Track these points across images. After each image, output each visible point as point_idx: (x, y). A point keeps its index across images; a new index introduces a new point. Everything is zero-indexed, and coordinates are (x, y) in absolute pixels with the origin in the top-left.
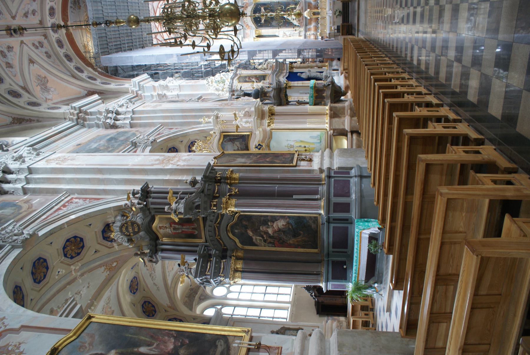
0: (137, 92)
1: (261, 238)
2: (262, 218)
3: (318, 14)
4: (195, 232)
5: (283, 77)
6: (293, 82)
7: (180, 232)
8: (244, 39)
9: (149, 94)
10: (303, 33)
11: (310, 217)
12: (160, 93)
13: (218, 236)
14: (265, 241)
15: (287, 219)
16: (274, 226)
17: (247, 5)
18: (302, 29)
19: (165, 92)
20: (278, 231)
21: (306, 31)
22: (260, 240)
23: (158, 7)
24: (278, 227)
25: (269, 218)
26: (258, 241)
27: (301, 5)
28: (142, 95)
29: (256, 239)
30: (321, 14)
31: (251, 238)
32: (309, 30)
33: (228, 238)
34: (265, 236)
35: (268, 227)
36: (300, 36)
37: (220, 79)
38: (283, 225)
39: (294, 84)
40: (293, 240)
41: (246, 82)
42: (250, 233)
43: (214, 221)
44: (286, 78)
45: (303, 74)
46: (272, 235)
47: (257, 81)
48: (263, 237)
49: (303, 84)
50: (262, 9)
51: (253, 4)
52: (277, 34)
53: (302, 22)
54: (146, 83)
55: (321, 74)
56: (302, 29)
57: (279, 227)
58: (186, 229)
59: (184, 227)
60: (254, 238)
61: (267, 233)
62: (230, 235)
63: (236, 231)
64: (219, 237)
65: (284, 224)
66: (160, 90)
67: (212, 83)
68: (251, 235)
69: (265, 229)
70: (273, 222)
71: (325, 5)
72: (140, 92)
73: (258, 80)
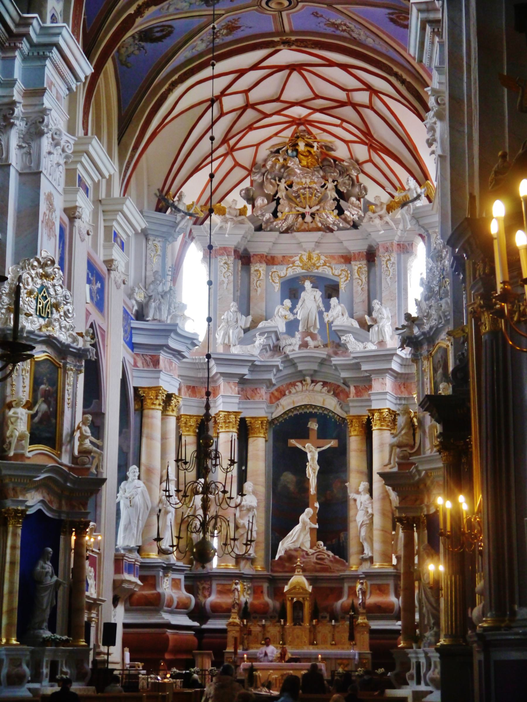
0: (27, 35)
3: (298, 620)
5: (42, 502)
6: (19, 531)
8: (237, 380)
9: (17, 74)
10: (246, 569)
12: (19, 110)
17: (342, 396)
18: (260, 567)
19: (20, 125)
21: (252, 579)
23: (343, 120)
27: (338, 566)
28: (17, 53)
30: (298, 630)
32: (256, 591)
36: (238, 559)
37: (53, 301)
39: (15, 535)
41: (36, 383)
44: (40, 511)
45: (48, 567)
47: (36, 419)
49: (12, 563)
50: (333, 443)
51: (344, 415)
52: (248, 486)
53: (284, 566)
54: (56, 66)
55: (45, 624)
56: (260, 567)
66: (30, 110)
67: (42, 276)
71: (325, 642)
72: (25, 46)
73: (41, 421)
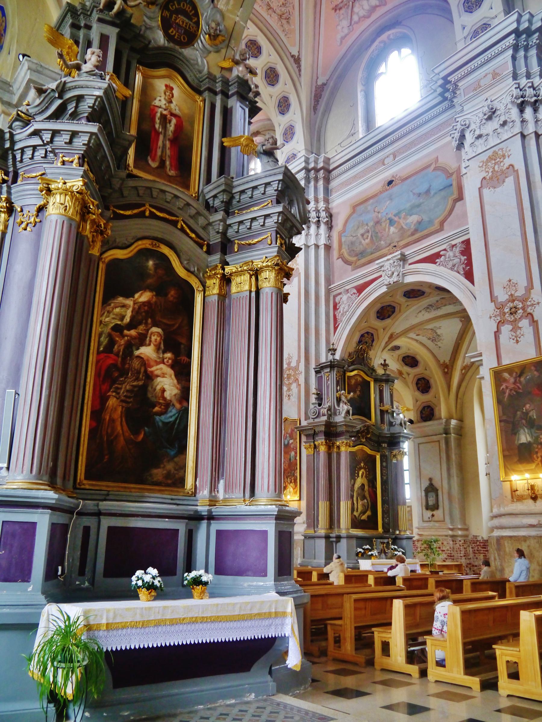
1: (127, 319)
2: (183, 341)
4: (153, 160)
7: (157, 126)
11: (183, 467)
13: (151, 212)
14: (117, 329)
15: (180, 402)
16: (162, 366)
20: (146, 371)
22: (122, 318)
24: (158, 376)
25: (184, 358)
26: (117, 310)
29: (124, 306)
31: (129, 294)
33: (140, 235)
34: (133, 332)
35: (158, 348)
38: (163, 390)
40: (120, 409)
42: (144, 297)
43: (191, 222)
46: (137, 353)
48: (130, 326)
57: (159, 379)
58: (164, 145)
59: (168, 144)
60: (129, 302)
61: (142, 341)
62: (146, 244)
63: (151, 263)
64: (147, 213)
65: (167, 395)
68: (136, 296)
69: (153, 338)
70: (172, 367)
